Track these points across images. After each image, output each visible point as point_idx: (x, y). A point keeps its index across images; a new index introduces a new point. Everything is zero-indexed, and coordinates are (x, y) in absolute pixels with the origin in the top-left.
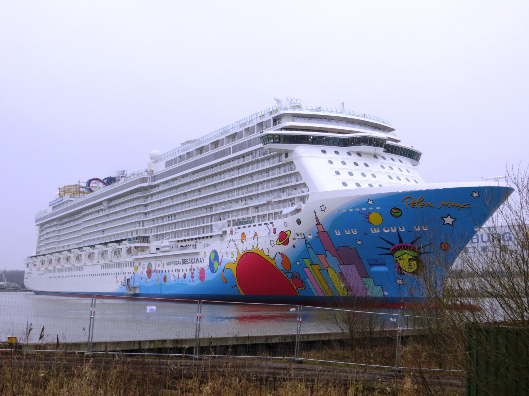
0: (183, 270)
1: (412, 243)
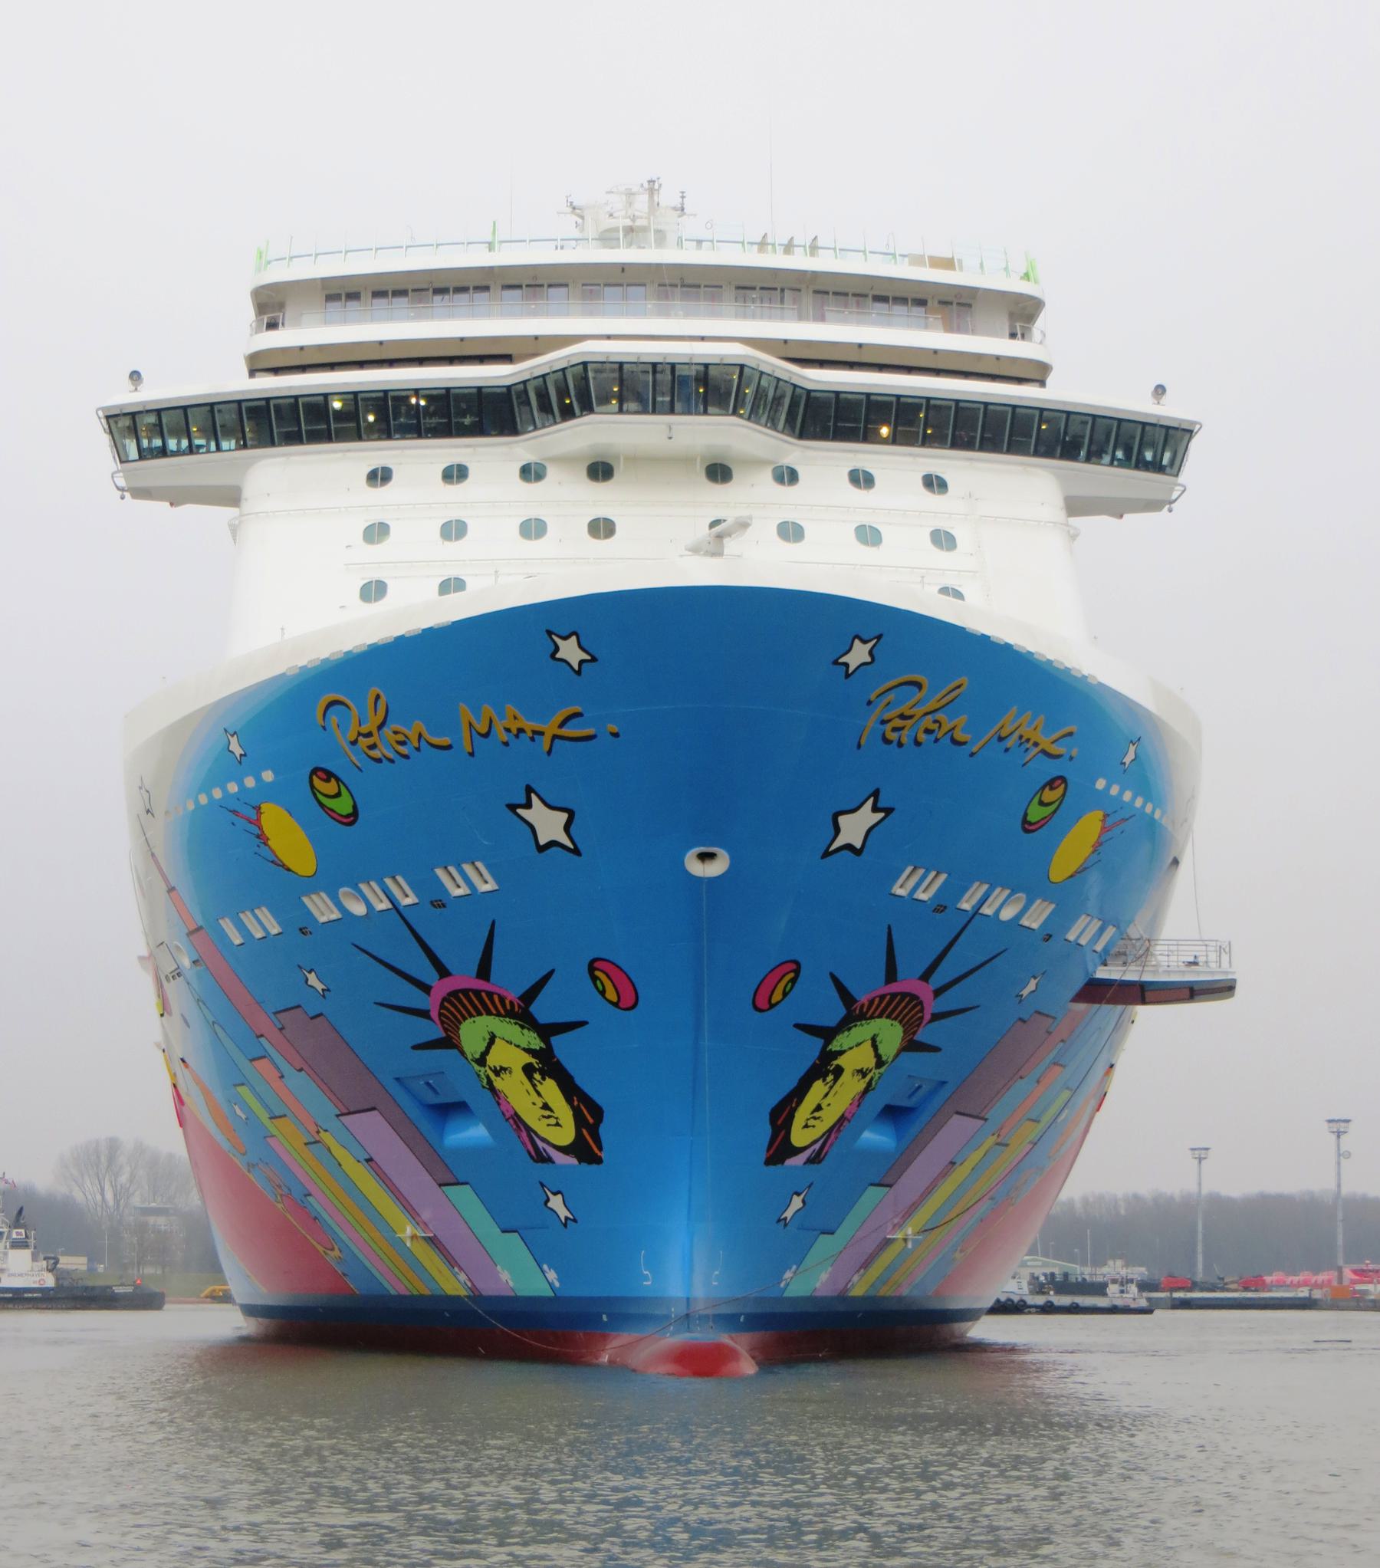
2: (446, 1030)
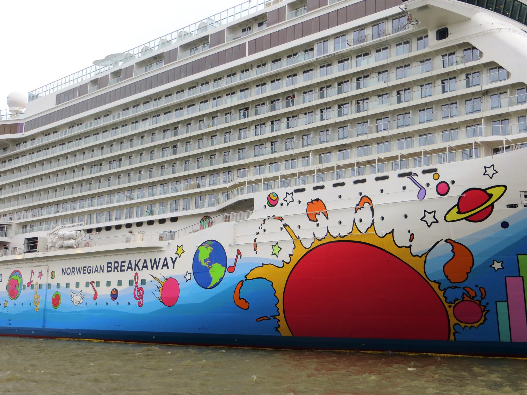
0: (108, 284)
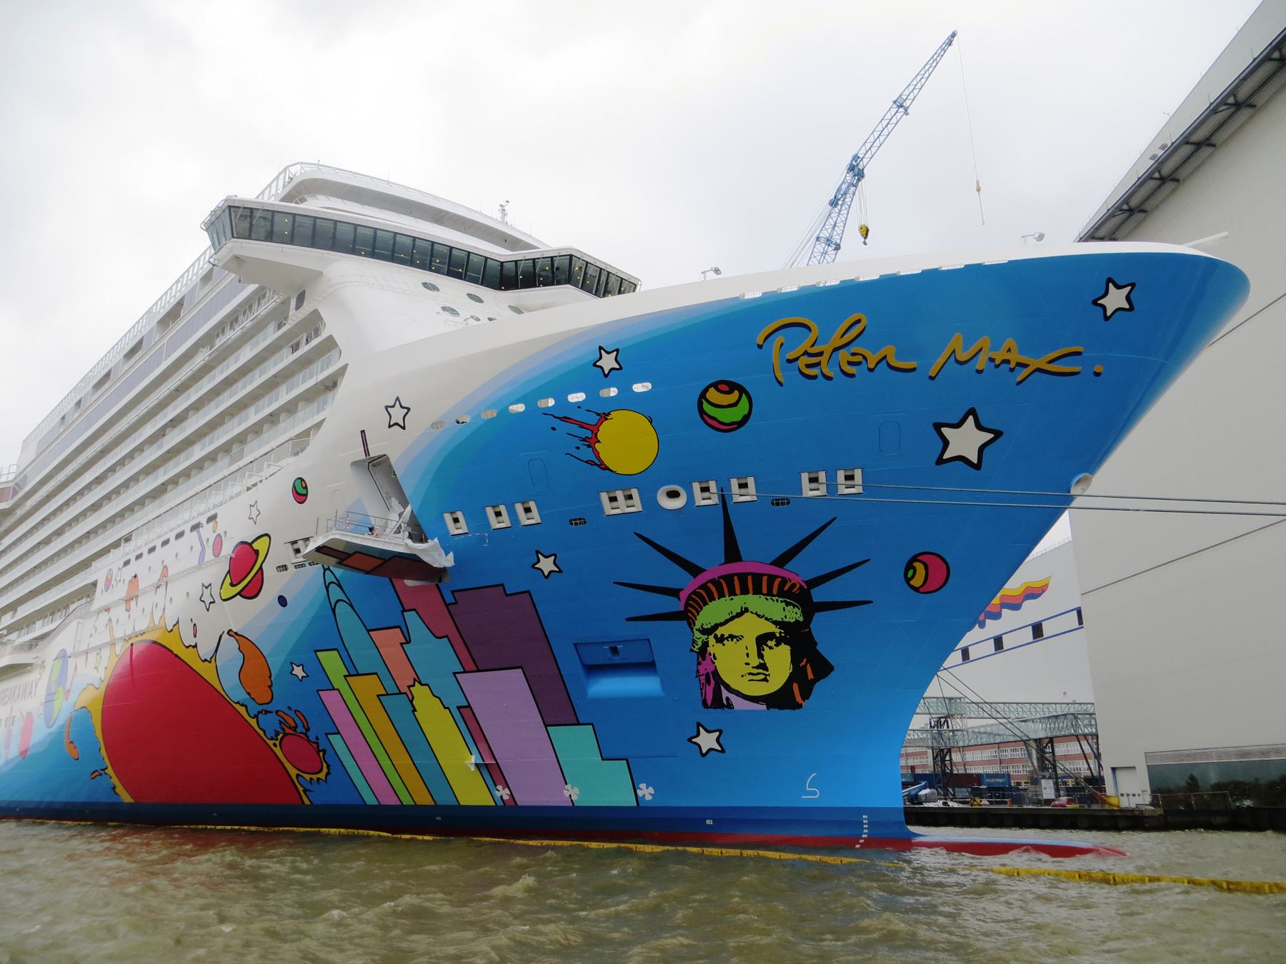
1: (781, 561)
2: (687, 604)
